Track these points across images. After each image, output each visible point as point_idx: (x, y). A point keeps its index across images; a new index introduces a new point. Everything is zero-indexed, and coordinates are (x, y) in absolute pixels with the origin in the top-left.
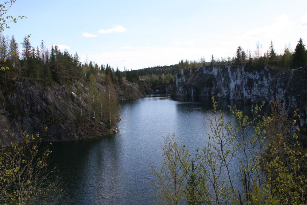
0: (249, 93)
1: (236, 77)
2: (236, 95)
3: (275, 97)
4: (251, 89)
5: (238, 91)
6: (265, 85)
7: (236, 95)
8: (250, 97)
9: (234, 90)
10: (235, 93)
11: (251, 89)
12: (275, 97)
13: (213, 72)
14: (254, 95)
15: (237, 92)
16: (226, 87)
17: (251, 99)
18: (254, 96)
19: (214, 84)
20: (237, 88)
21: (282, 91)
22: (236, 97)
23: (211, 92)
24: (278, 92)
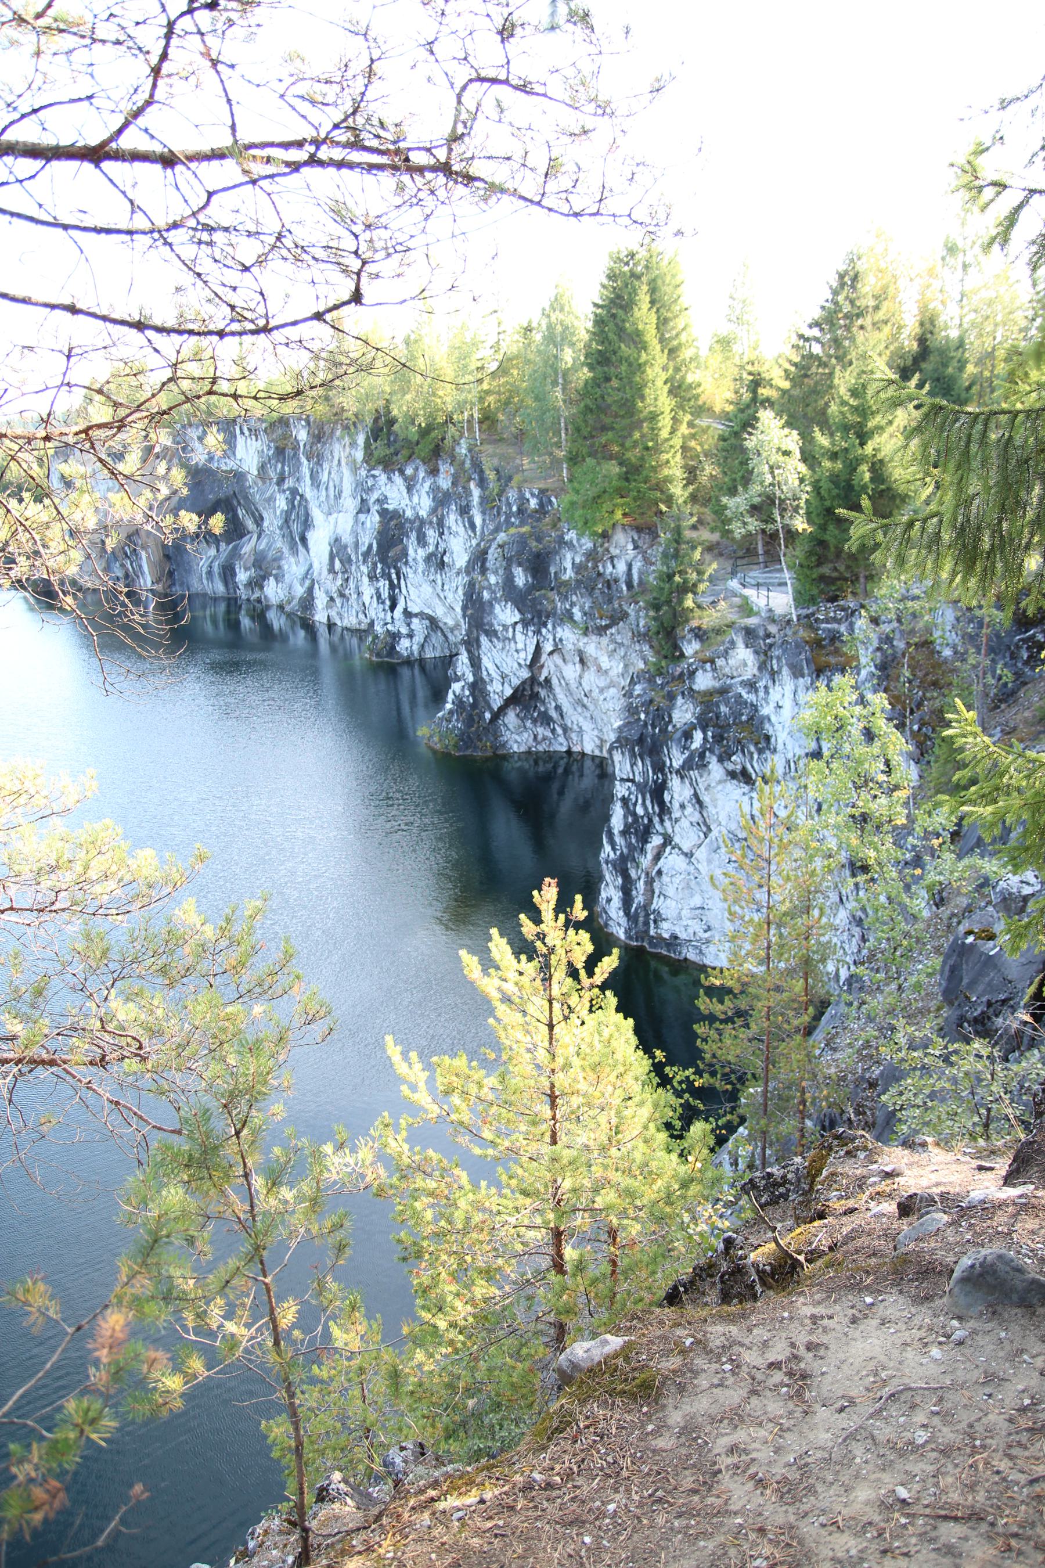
0: (388, 603)
2: (338, 601)
3: (476, 663)
4: (394, 576)
7: (338, 601)
8: (389, 627)
9: (325, 572)
10: (334, 589)
11: (394, 576)
12: (476, 663)
14: (416, 615)
15: (339, 582)
16: (300, 547)
17: (395, 636)
19: (250, 524)
22: (339, 614)
23: (234, 574)
24: (491, 634)
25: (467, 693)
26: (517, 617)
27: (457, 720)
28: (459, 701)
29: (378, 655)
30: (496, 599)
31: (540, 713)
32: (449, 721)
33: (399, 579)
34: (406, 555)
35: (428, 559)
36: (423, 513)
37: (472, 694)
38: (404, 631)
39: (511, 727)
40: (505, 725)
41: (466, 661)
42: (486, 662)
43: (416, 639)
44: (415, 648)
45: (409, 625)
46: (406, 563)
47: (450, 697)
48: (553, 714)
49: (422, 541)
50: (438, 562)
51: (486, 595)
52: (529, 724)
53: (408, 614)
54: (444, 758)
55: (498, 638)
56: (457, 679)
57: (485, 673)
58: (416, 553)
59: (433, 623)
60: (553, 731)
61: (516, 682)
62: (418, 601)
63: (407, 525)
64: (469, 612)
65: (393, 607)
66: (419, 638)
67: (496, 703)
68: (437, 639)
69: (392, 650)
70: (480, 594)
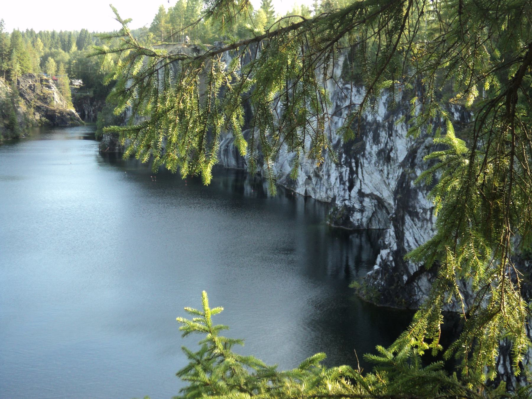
0: (347, 184)
2: (314, 180)
4: (354, 164)
7: (314, 180)
8: (347, 202)
10: (312, 171)
11: (354, 164)
12: (400, 236)
14: (367, 196)
17: (350, 210)
18: (367, 200)
22: (313, 189)
24: (414, 215)
25: (391, 258)
27: (381, 279)
28: (384, 264)
29: (336, 223)
30: (420, 188)
32: (375, 279)
33: (357, 167)
34: (363, 148)
35: (379, 154)
36: (380, 119)
37: (394, 260)
38: (357, 206)
39: (423, 289)
40: (419, 287)
41: (393, 233)
42: (408, 236)
43: (366, 214)
44: (364, 220)
45: (361, 202)
46: (364, 156)
47: (379, 260)
49: (376, 140)
50: (385, 156)
51: (412, 183)
53: (361, 194)
54: (369, 307)
55: (419, 219)
56: (385, 247)
57: (406, 245)
58: (372, 149)
59: (380, 203)
62: (370, 185)
63: (368, 127)
64: (399, 196)
65: (351, 188)
66: (368, 213)
67: (413, 268)
69: (346, 220)
70: (408, 185)
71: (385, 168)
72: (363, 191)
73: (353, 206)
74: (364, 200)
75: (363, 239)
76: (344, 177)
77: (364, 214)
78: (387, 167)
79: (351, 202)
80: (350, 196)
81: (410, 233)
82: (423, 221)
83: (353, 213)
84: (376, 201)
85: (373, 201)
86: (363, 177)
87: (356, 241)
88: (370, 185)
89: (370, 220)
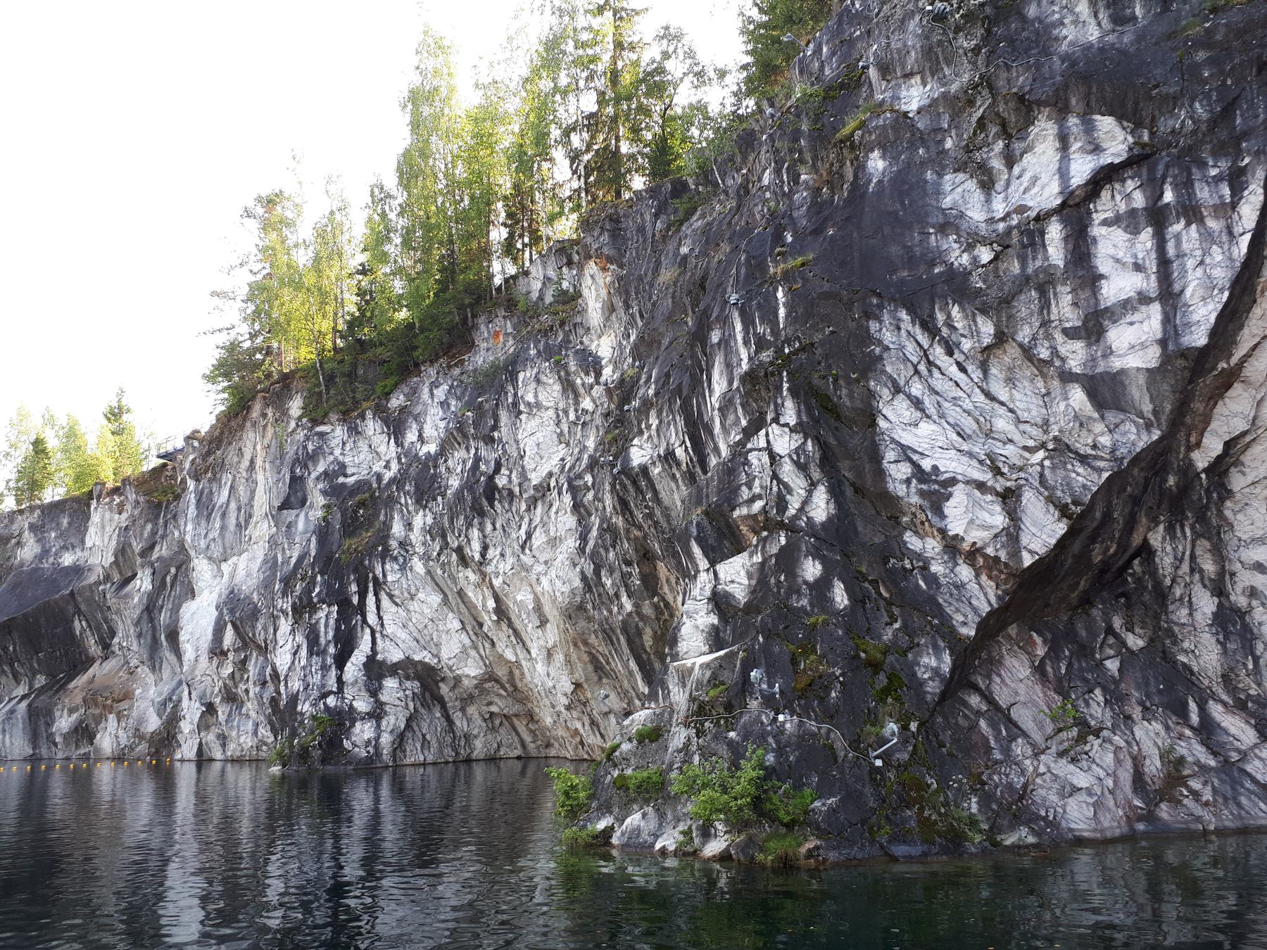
0: (332, 650)
1: (232, 521)
2: (222, 711)
5: (242, 665)
6: (535, 478)
8: (331, 701)
11: (354, 588)
12: (844, 440)
13: (89, 543)
14: (393, 670)
15: (228, 669)
20: (229, 636)
21: (1075, 209)
25: (811, 570)
26: (1115, 140)
31: (1128, 657)
38: (362, 705)
39: (1023, 717)
40: (1001, 715)
43: (389, 722)
44: (386, 739)
45: (374, 693)
48: (1205, 655)
52: (1097, 709)
53: (376, 670)
60: (1207, 731)
61: (1086, 480)
62: (402, 635)
66: (394, 720)
68: (431, 724)
71: (475, 533)
72: (379, 657)
73: (351, 706)
74: (381, 687)
75: (385, 791)
76: (322, 634)
77: (384, 723)
78: (482, 530)
79: (343, 698)
80: (340, 680)
81: (917, 403)
82: (1007, 301)
83: (353, 725)
84: (417, 684)
85: (408, 684)
86: (380, 618)
87: (360, 798)
88: (402, 635)
89: (400, 740)
